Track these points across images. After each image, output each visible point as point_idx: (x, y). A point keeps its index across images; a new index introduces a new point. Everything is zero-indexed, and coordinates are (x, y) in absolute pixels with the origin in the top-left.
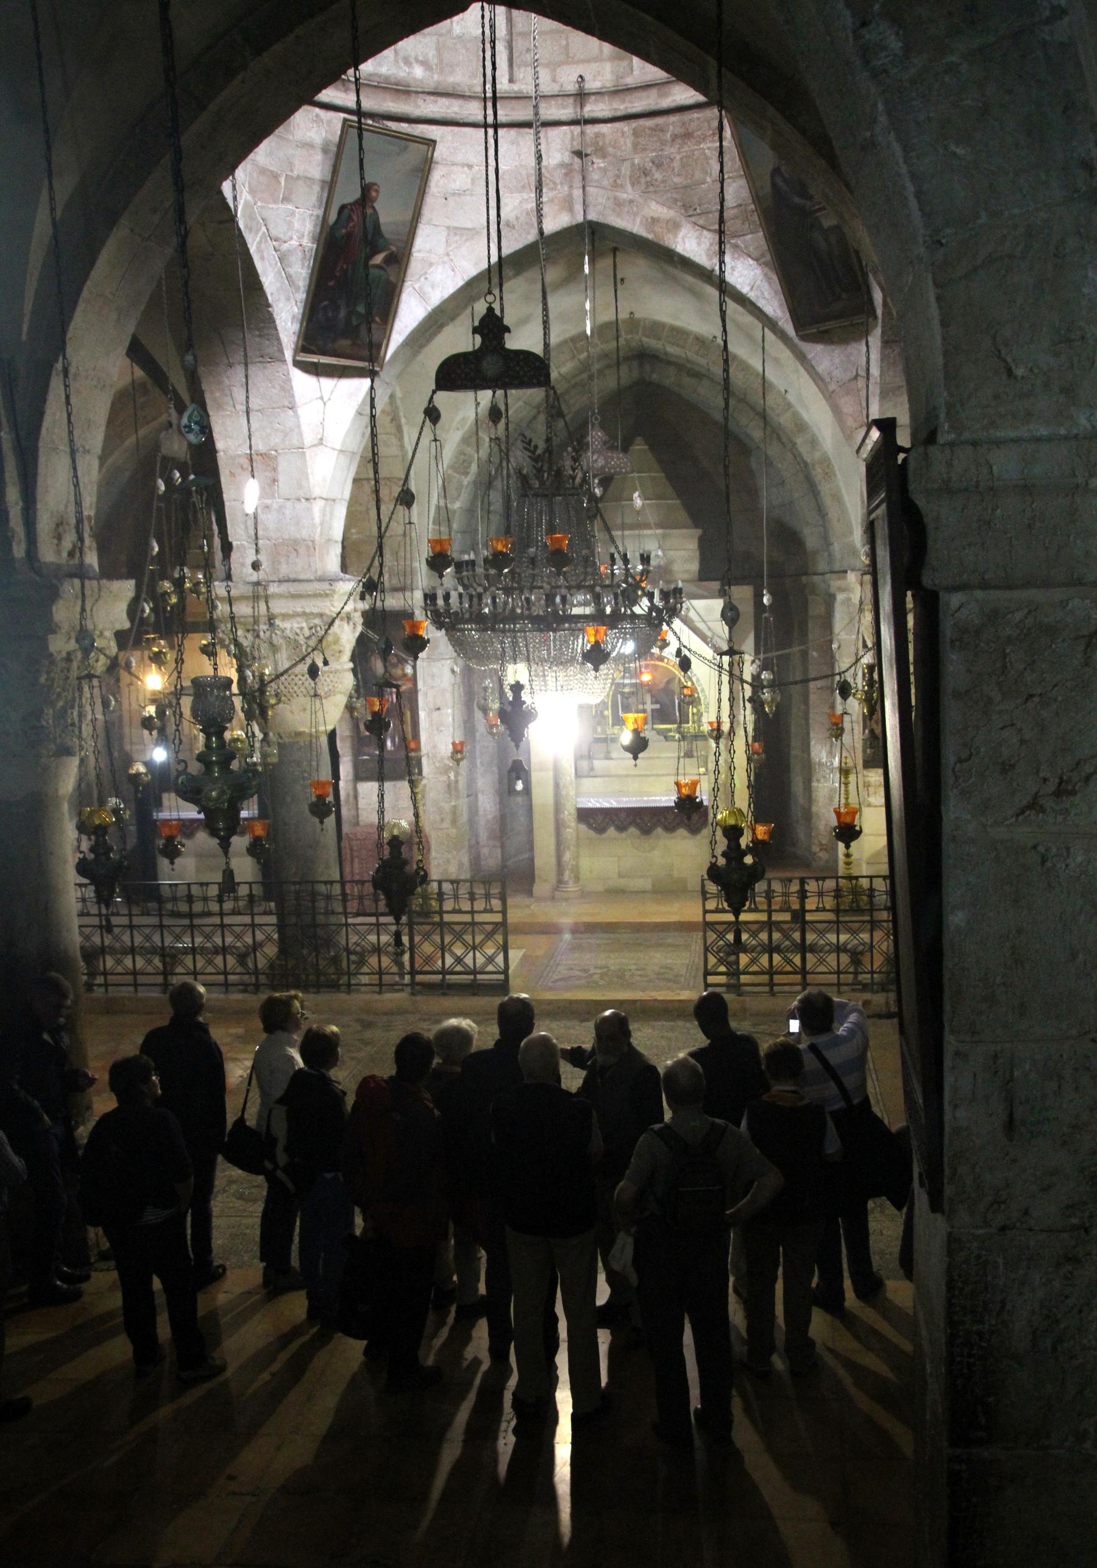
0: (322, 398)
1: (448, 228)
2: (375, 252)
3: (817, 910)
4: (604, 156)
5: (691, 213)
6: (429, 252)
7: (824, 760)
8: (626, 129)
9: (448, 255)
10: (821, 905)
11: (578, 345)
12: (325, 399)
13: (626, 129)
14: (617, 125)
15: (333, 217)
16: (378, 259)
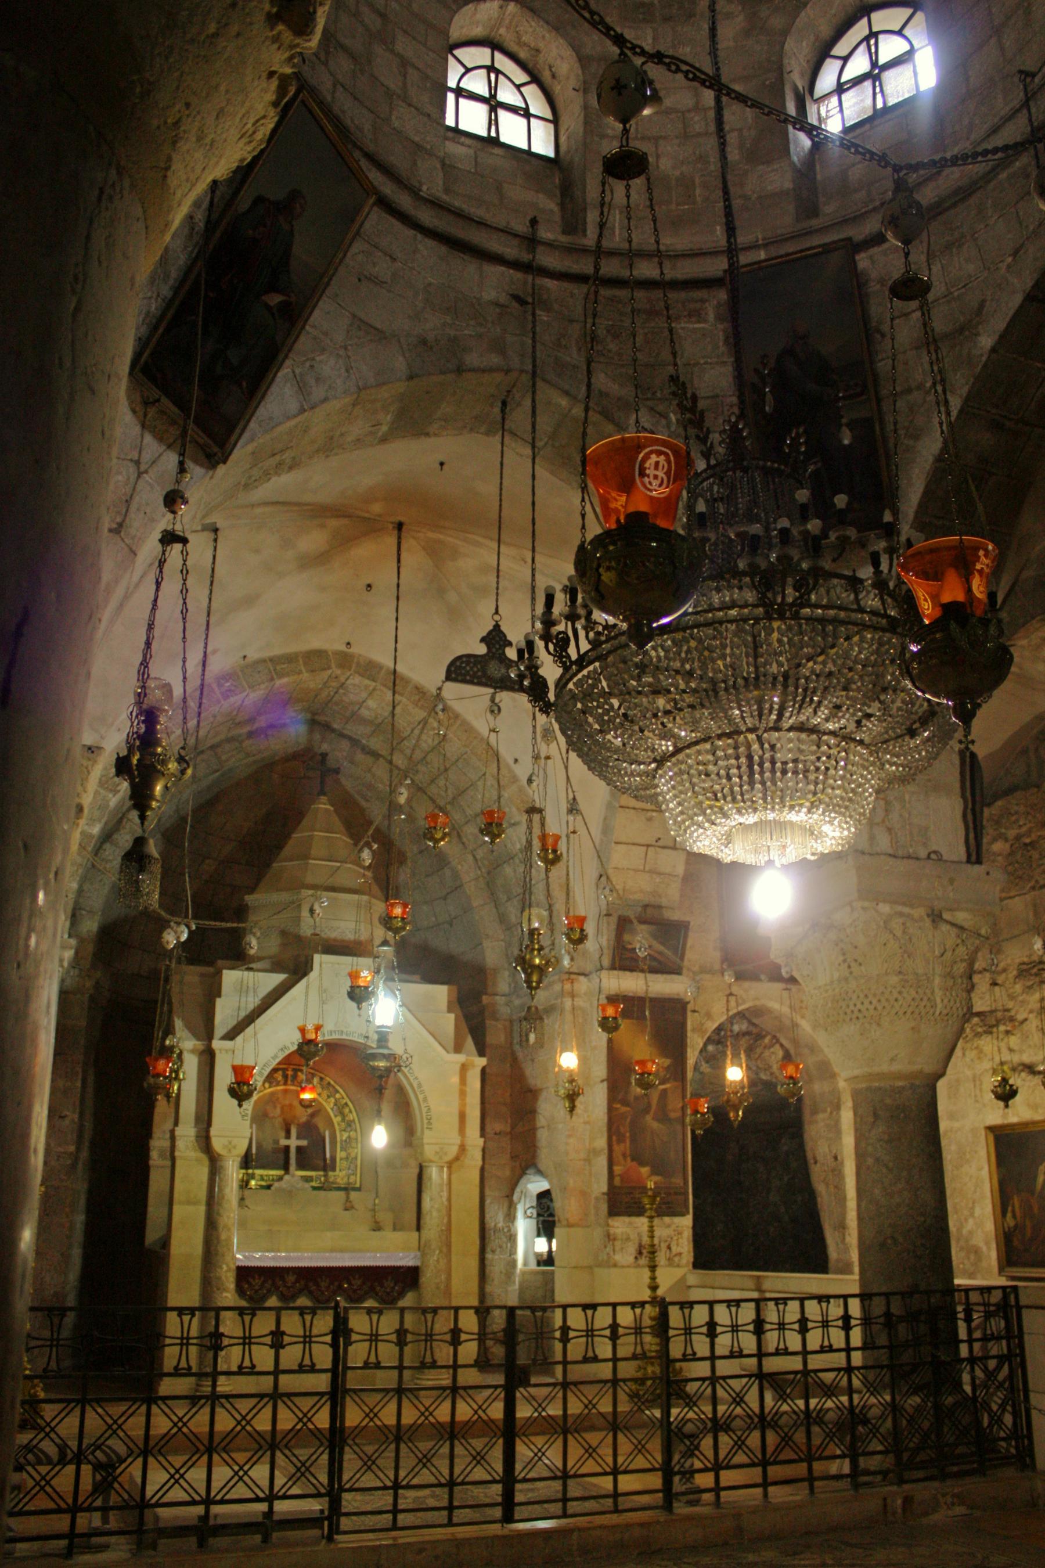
0: (137, 463)
1: (354, 316)
2: (273, 288)
3: (822, 1350)
4: (548, 310)
5: (649, 395)
6: (326, 334)
7: (500, 1225)
8: (576, 291)
9: (346, 349)
10: (826, 1343)
11: (278, 668)
12: (143, 468)
13: (576, 291)
14: (566, 285)
15: (244, 204)
16: (275, 299)
